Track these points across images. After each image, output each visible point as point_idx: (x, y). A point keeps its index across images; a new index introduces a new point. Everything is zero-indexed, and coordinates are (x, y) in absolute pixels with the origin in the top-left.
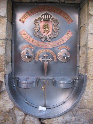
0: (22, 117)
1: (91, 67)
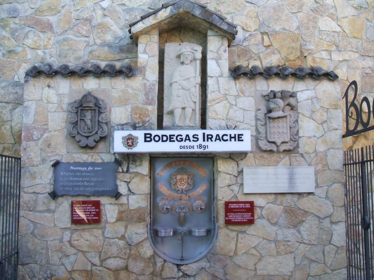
0: (161, 263)
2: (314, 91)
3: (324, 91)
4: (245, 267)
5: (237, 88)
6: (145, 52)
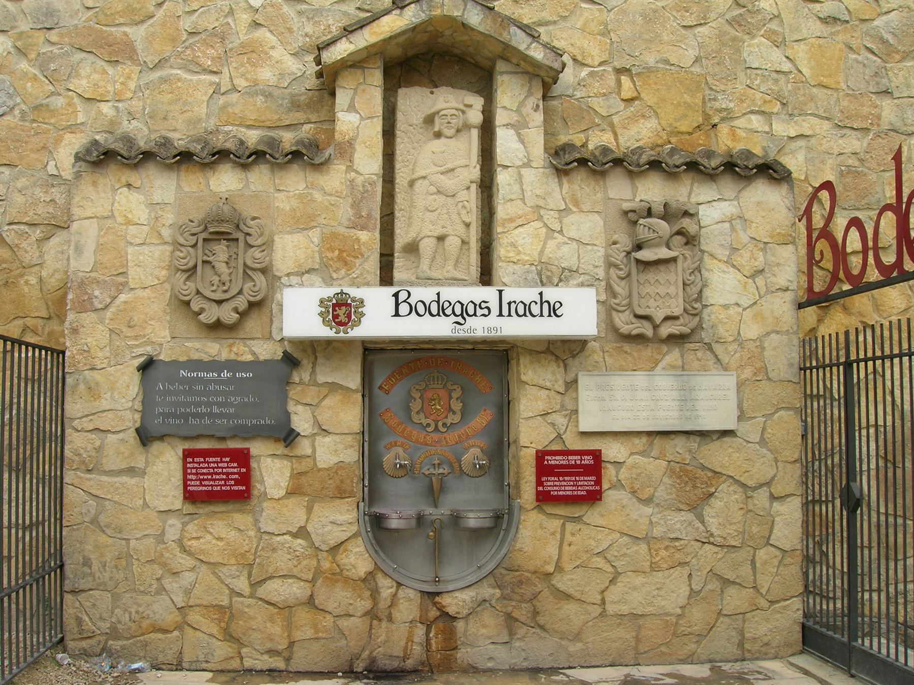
1: (528, 484)
2: (735, 203)
3: (759, 204)
4: (579, 597)
5: (564, 192)
6: (352, 108)
